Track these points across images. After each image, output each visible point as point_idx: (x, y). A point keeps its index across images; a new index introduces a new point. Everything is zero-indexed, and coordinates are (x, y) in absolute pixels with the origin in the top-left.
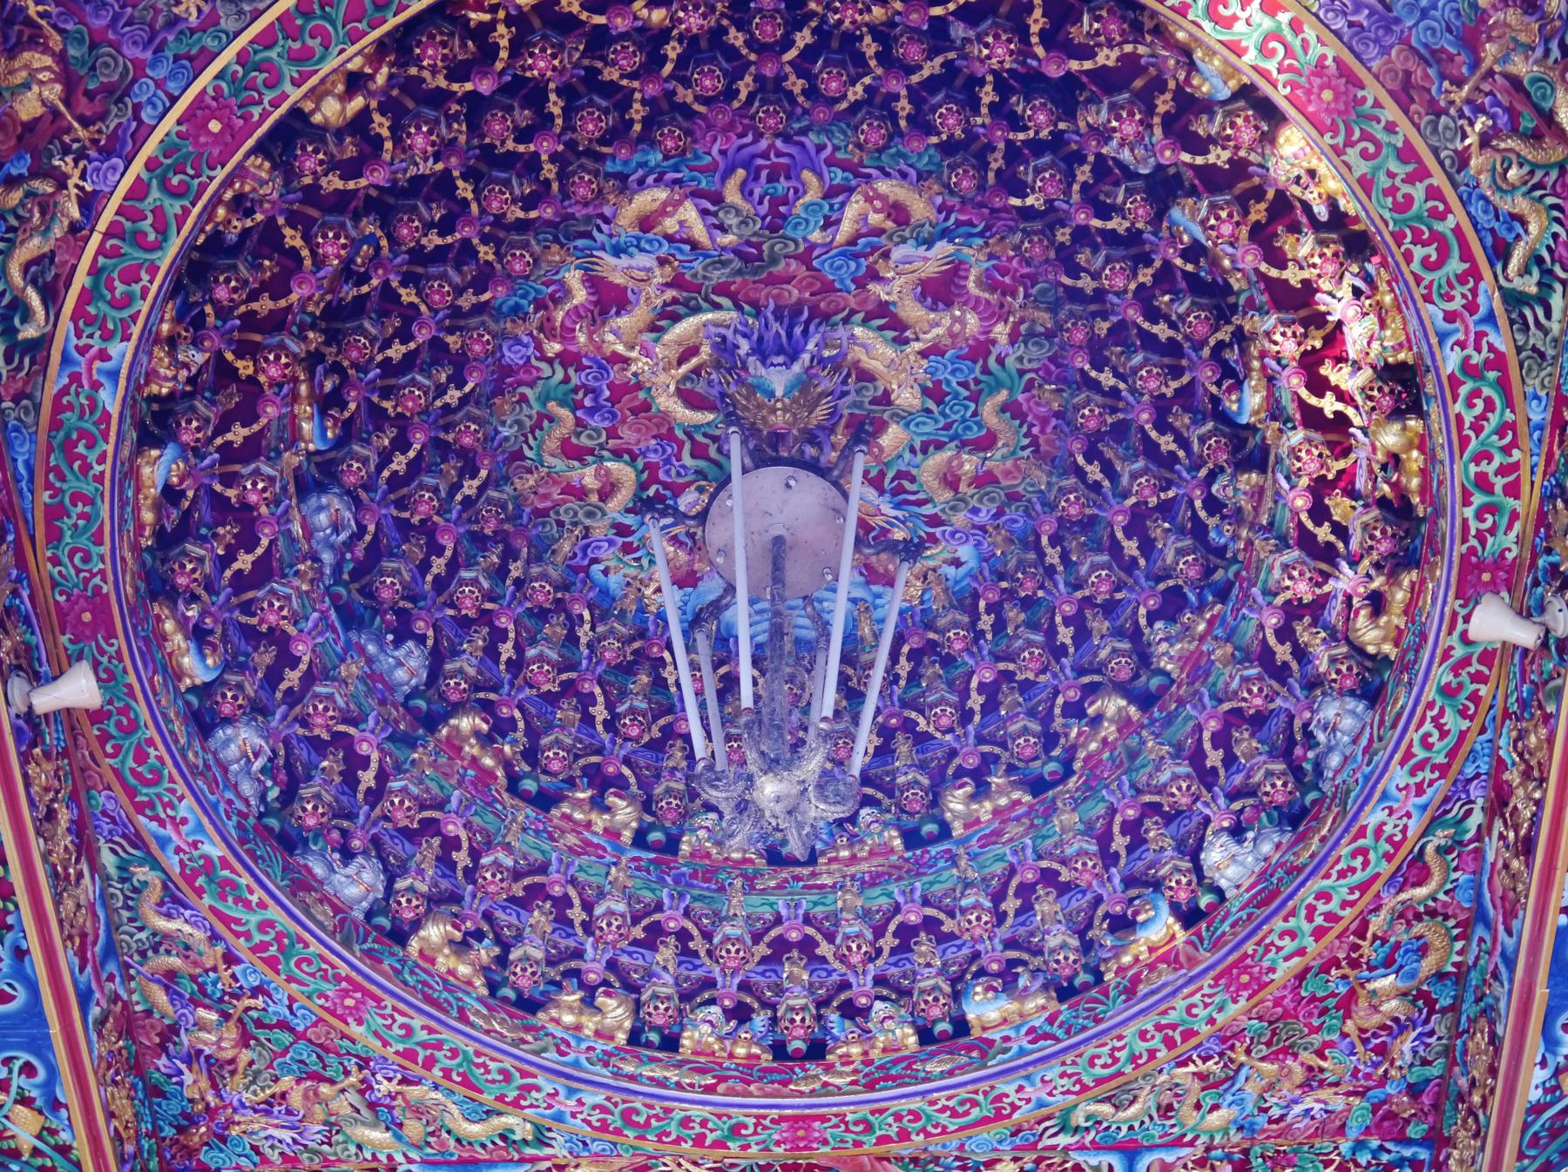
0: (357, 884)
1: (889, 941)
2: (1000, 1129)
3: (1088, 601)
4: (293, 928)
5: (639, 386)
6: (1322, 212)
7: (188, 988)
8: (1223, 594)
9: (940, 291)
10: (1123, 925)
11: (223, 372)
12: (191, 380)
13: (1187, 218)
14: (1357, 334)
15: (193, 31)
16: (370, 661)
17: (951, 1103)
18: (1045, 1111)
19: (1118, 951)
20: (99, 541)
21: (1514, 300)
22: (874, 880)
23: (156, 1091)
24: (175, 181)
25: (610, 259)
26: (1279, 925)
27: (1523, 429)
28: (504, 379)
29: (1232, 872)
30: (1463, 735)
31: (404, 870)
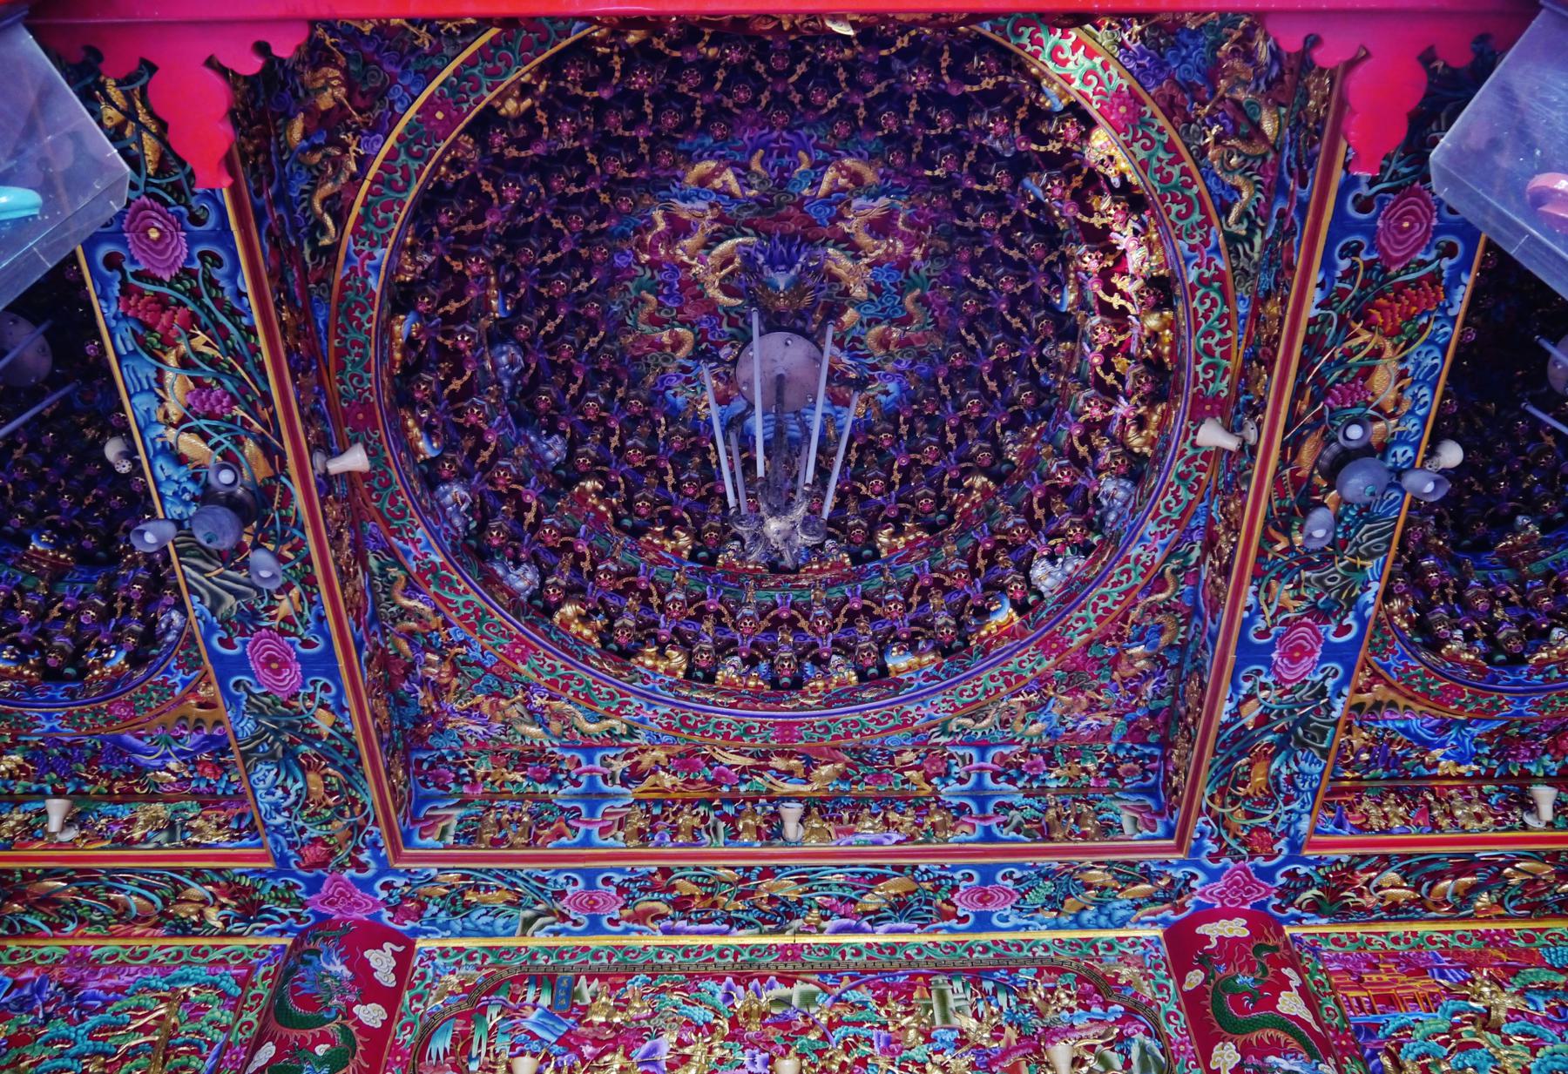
0: (523, 580)
1: (841, 620)
2: (906, 733)
3: (966, 418)
4: (485, 606)
5: (697, 282)
6: (1116, 181)
7: (421, 641)
8: (1047, 416)
9: (881, 227)
10: (983, 613)
11: (442, 268)
12: (424, 273)
13: (1034, 186)
14: (1135, 258)
16: (532, 446)
19: (979, 628)
20: (368, 370)
21: (1232, 239)
22: (834, 583)
23: (401, 702)
26: (1076, 614)
28: (615, 277)
29: (1049, 582)
30: (1190, 502)
31: (551, 573)
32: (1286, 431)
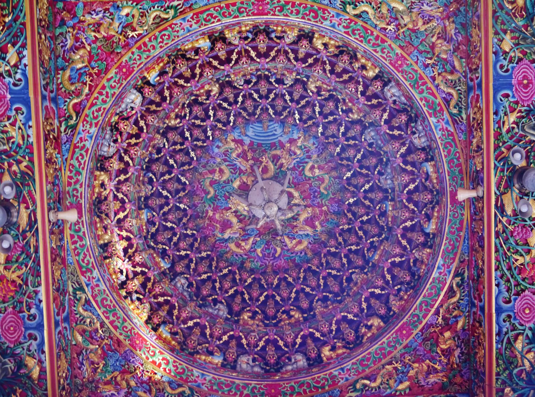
15: (407, 353)
17: (213, 20)
18: (182, 17)
24: (416, 319)
27: (73, 254)
32: (37, 229)
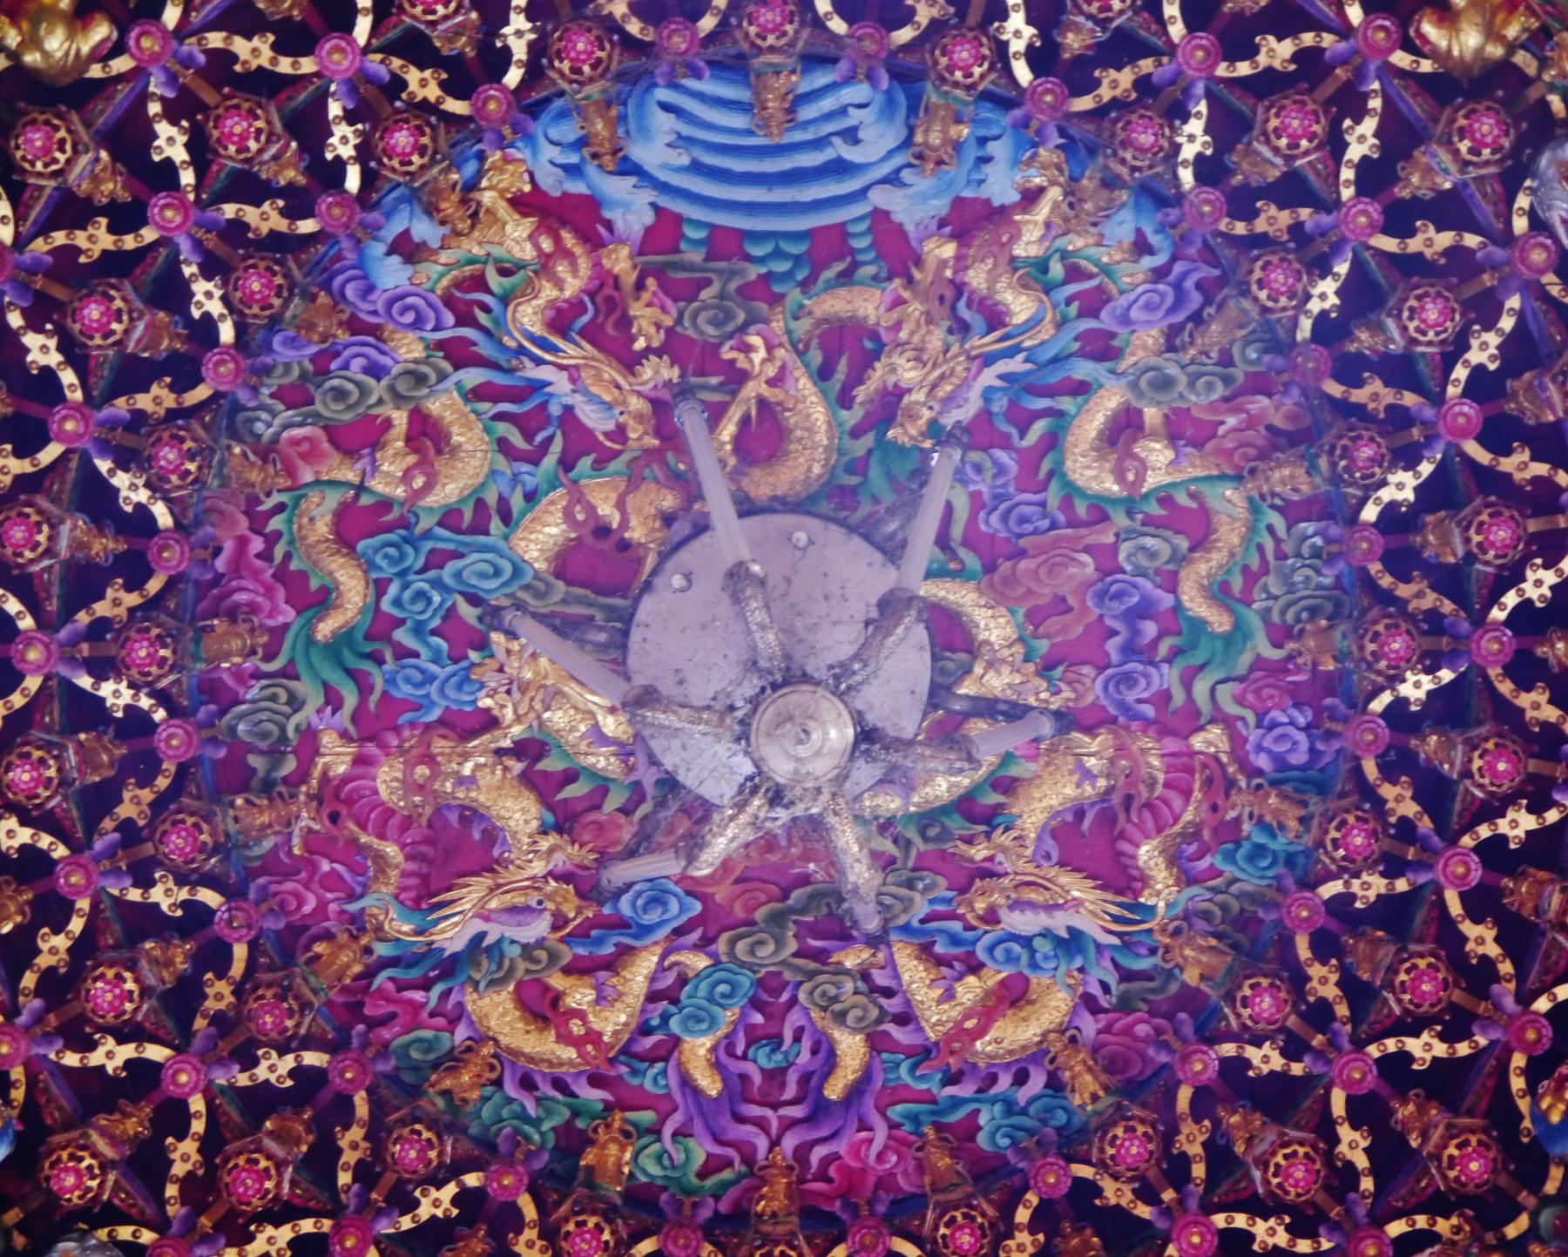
25: (1091, 927)
